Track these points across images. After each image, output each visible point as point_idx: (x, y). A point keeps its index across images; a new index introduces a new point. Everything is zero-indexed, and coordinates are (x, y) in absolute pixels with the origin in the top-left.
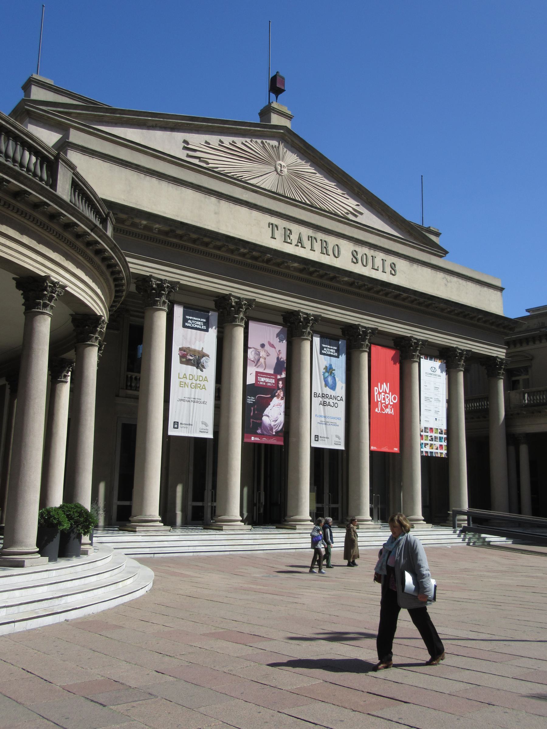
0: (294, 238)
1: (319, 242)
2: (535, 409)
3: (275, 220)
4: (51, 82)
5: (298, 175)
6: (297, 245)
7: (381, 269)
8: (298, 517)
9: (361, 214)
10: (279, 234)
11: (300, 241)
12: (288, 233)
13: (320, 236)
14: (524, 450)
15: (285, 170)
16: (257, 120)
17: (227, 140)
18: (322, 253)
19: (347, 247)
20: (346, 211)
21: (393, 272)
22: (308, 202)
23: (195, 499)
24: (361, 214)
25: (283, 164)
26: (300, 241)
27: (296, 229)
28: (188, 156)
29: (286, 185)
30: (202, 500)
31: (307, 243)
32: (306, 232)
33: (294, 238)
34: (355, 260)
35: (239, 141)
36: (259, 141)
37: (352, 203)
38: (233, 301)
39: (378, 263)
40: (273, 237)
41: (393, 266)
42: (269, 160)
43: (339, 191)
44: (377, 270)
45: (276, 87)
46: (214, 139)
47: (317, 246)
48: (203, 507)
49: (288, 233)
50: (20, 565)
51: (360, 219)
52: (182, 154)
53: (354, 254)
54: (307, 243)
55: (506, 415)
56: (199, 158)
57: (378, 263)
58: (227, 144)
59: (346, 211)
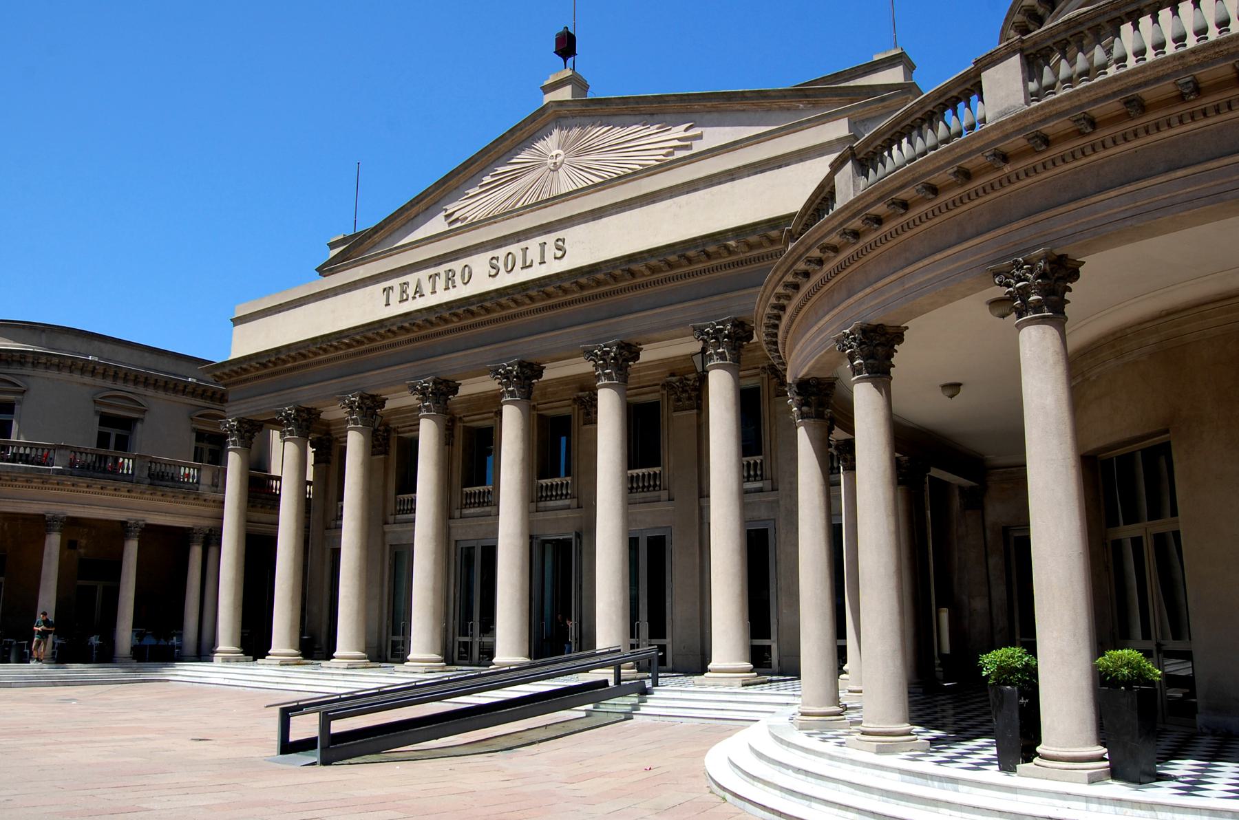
0: (411, 291)
1: (443, 276)
6: (414, 298)
7: (537, 260)
9: (700, 137)
10: (395, 296)
13: (442, 269)
18: (447, 288)
19: (480, 263)
20: (664, 152)
21: (559, 254)
22: (597, 180)
23: (632, 636)
24: (700, 137)
25: (554, 153)
27: (411, 278)
28: (450, 224)
32: (423, 275)
33: (411, 291)
34: (493, 272)
37: (679, 131)
40: (387, 304)
43: (653, 129)
44: (530, 266)
47: (441, 283)
52: (445, 227)
59: (664, 152)
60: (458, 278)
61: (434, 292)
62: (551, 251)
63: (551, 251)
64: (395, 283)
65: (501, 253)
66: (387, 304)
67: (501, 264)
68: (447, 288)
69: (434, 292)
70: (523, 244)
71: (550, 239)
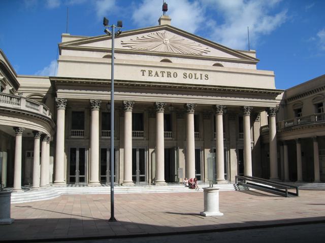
0: (154, 73)
1: (166, 73)
2: (288, 129)
3: (143, 68)
4: (69, 34)
5: (174, 42)
7: (200, 78)
8: (158, 181)
10: (146, 74)
11: (157, 74)
12: (150, 73)
13: (166, 70)
14: (285, 147)
15: (168, 42)
16: (158, 25)
17: (140, 36)
18: (168, 77)
19: (180, 73)
26: (157, 74)
27: (154, 70)
29: (169, 48)
30: (105, 174)
31: (160, 75)
32: (159, 70)
33: (154, 73)
35: (145, 35)
36: (155, 33)
37: (204, 47)
38: (125, 103)
39: (198, 76)
41: (207, 76)
42: (161, 40)
45: (165, 8)
46: (134, 37)
47: (165, 75)
48: (144, 177)
49: (150, 73)
50: (16, 192)
51: (209, 55)
53: (185, 75)
54: (160, 75)
55: (277, 132)
56: (128, 46)
57: (198, 76)
58: (140, 38)
60: (172, 75)
61: (163, 76)
62: (204, 77)
63: (204, 77)
64: (147, 69)
65: (188, 72)
66: (143, 75)
67: (188, 75)
68: (168, 77)
69: (163, 76)
70: (195, 72)
71: (204, 73)
